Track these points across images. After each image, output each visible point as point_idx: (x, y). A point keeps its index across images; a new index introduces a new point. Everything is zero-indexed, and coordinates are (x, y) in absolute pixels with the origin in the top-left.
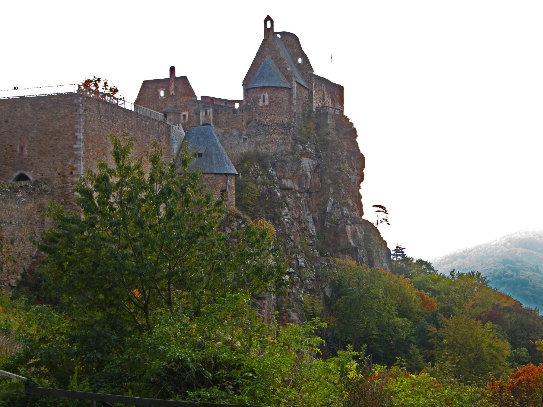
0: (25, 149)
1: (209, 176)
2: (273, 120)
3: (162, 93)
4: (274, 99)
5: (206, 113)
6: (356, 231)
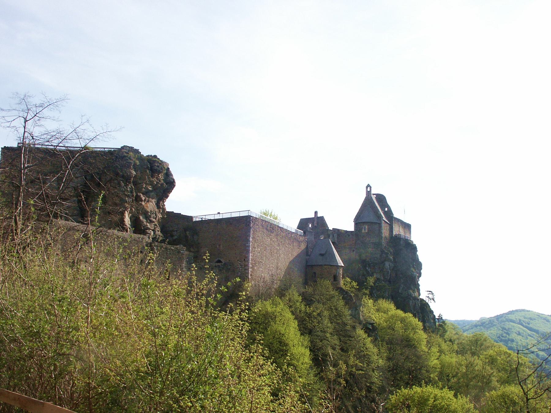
0: (221, 246)
1: (327, 266)
3: (310, 226)
5: (333, 236)
6: (416, 304)
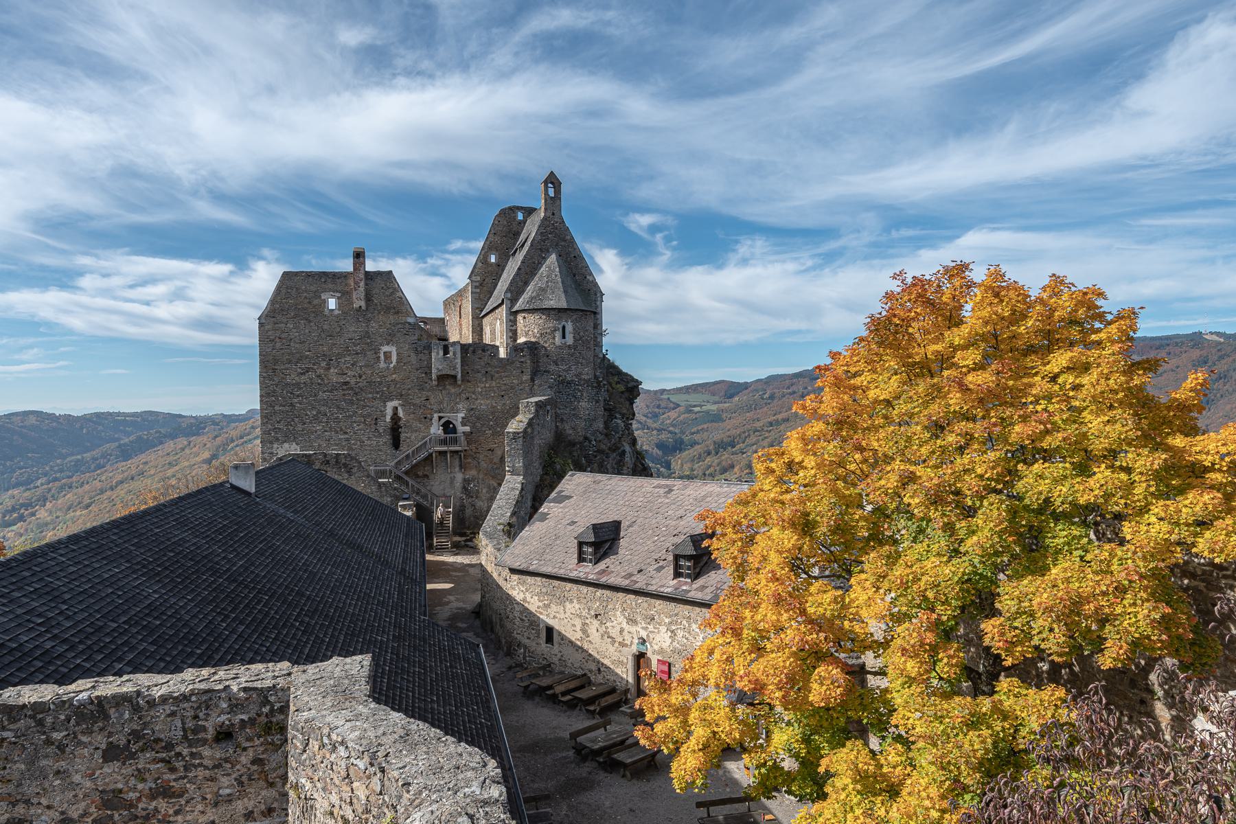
2: (581, 373)
3: (332, 304)
4: (582, 334)
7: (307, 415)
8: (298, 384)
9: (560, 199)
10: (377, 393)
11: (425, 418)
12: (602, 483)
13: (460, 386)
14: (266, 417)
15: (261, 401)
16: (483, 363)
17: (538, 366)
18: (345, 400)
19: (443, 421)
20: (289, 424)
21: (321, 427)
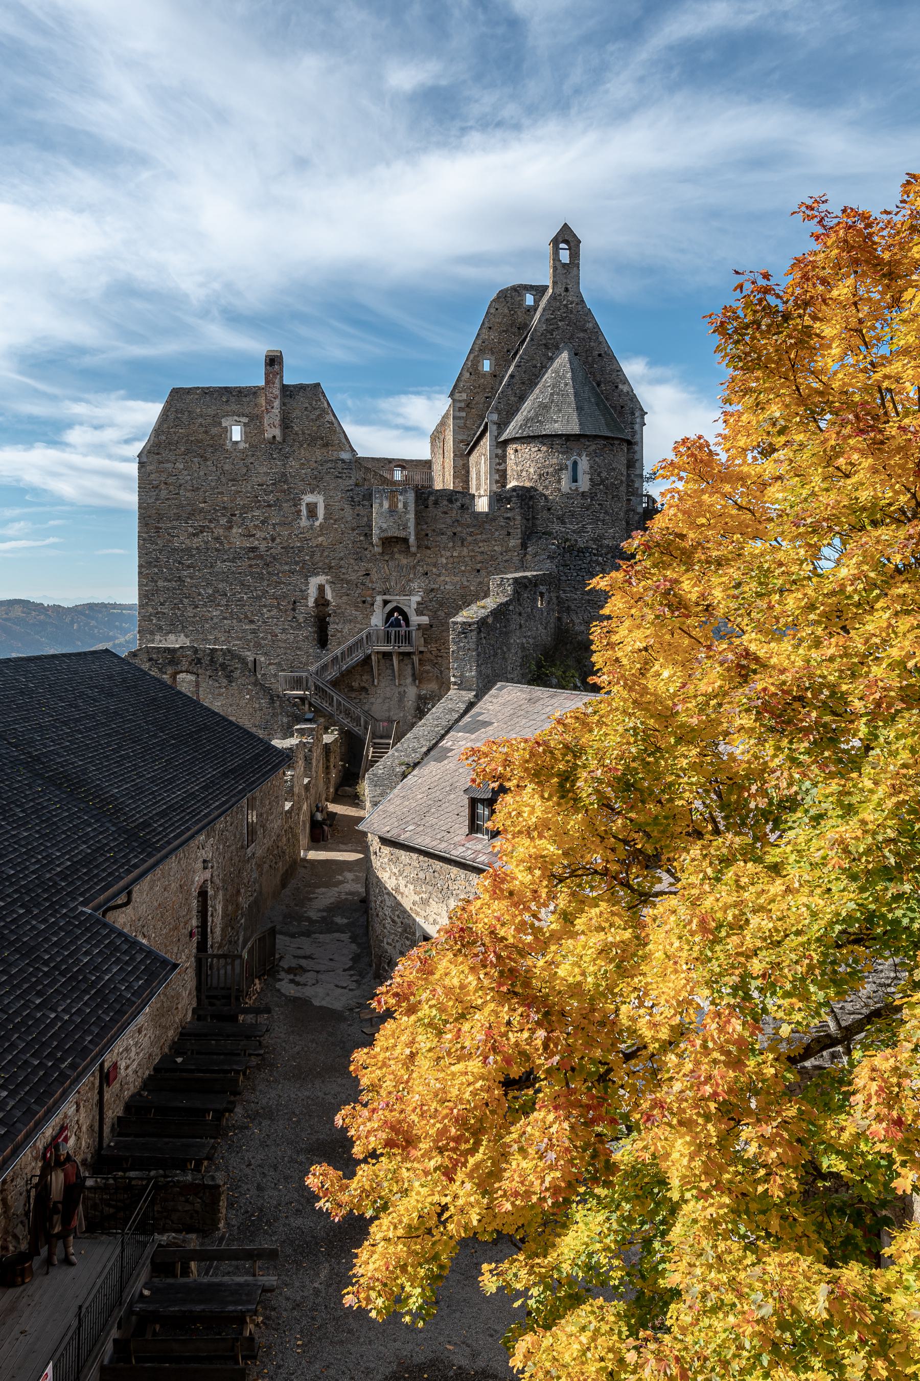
2: (601, 537)
3: (237, 433)
4: (604, 475)
7: (200, 594)
8: (188, 550)
9: (578, 266)
10: (297, 563)
11: (364, 602)
12: (541, 702)
13: (415, 554)
14: (146, 596)
15: (140, 573)
16: (449, 521)
17: (534, 525)
18: (251, 574)
19: (390, 607)
20: (175, 607)
21: (218, 613)
